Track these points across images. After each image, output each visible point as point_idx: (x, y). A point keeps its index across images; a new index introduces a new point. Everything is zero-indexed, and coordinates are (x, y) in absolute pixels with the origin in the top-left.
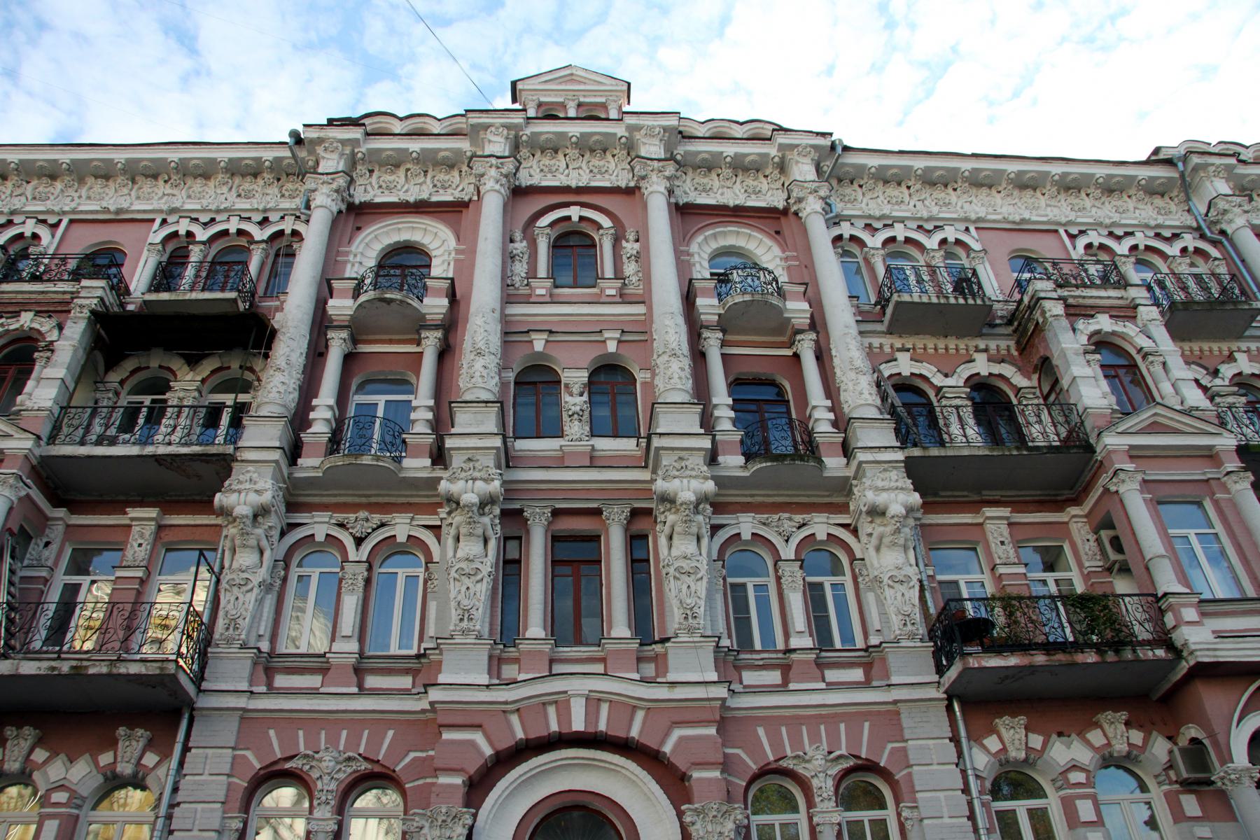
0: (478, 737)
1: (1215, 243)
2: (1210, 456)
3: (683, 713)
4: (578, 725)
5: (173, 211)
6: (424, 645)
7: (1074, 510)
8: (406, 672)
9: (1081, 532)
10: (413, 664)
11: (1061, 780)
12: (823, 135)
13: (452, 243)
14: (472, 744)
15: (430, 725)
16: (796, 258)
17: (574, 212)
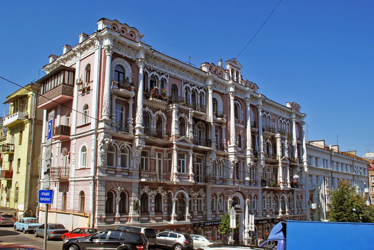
0: (232, 191)
1: (290, 123)
2: (287, 164)
3: (245, 189)
4: (239, 190)
5: (186, 80)
6: (224, 178)
7: (273, 165)
8: (222, 180)
9: (272, 168)
10: (222, 179)
11: (267, 198)
12: (265, 96)
13: (221, 102)
14: (231, 192)
15: (227, 189)
16: (255, 116)
17: (237, 102)
